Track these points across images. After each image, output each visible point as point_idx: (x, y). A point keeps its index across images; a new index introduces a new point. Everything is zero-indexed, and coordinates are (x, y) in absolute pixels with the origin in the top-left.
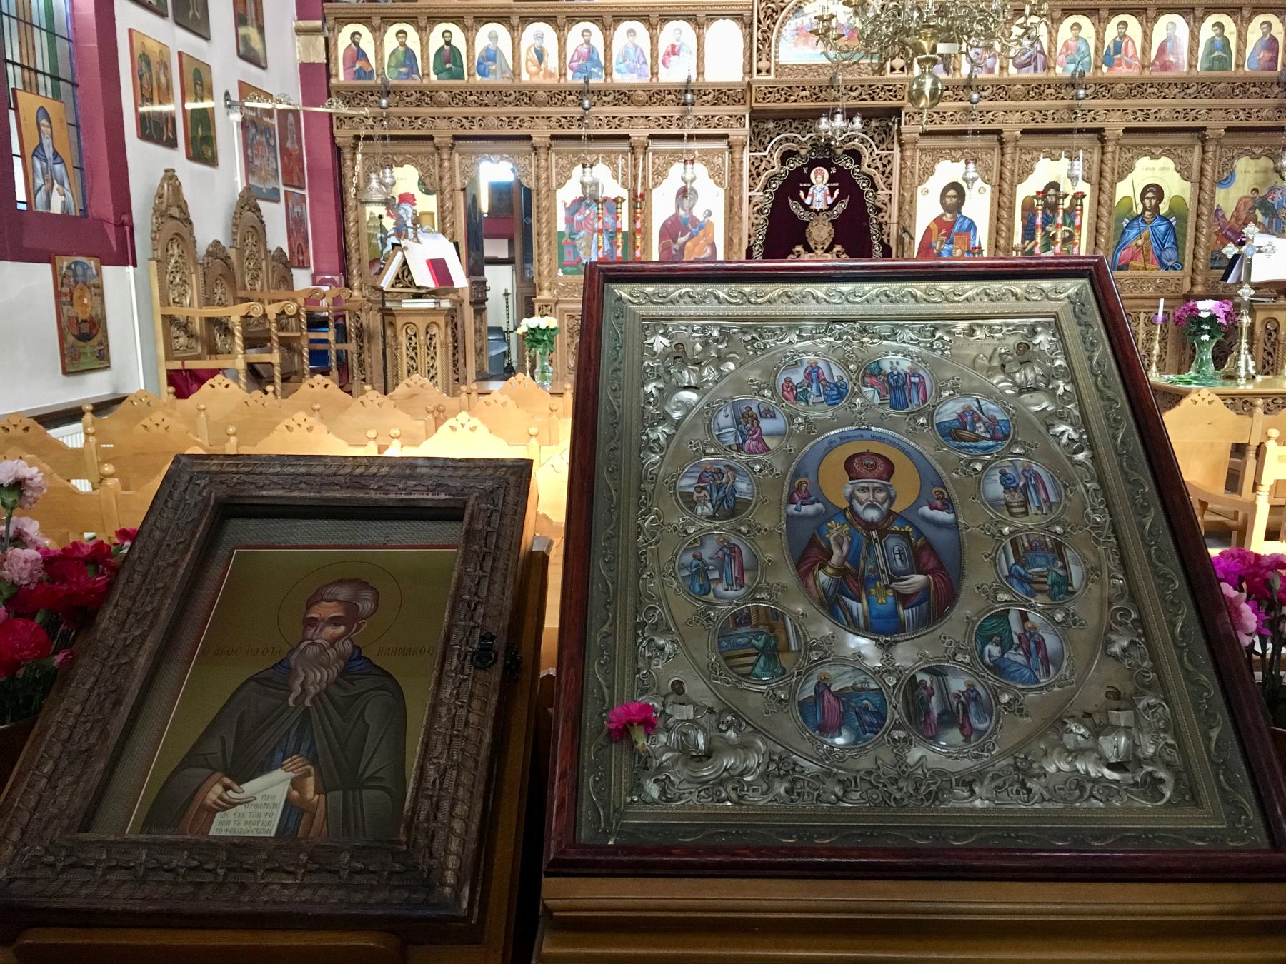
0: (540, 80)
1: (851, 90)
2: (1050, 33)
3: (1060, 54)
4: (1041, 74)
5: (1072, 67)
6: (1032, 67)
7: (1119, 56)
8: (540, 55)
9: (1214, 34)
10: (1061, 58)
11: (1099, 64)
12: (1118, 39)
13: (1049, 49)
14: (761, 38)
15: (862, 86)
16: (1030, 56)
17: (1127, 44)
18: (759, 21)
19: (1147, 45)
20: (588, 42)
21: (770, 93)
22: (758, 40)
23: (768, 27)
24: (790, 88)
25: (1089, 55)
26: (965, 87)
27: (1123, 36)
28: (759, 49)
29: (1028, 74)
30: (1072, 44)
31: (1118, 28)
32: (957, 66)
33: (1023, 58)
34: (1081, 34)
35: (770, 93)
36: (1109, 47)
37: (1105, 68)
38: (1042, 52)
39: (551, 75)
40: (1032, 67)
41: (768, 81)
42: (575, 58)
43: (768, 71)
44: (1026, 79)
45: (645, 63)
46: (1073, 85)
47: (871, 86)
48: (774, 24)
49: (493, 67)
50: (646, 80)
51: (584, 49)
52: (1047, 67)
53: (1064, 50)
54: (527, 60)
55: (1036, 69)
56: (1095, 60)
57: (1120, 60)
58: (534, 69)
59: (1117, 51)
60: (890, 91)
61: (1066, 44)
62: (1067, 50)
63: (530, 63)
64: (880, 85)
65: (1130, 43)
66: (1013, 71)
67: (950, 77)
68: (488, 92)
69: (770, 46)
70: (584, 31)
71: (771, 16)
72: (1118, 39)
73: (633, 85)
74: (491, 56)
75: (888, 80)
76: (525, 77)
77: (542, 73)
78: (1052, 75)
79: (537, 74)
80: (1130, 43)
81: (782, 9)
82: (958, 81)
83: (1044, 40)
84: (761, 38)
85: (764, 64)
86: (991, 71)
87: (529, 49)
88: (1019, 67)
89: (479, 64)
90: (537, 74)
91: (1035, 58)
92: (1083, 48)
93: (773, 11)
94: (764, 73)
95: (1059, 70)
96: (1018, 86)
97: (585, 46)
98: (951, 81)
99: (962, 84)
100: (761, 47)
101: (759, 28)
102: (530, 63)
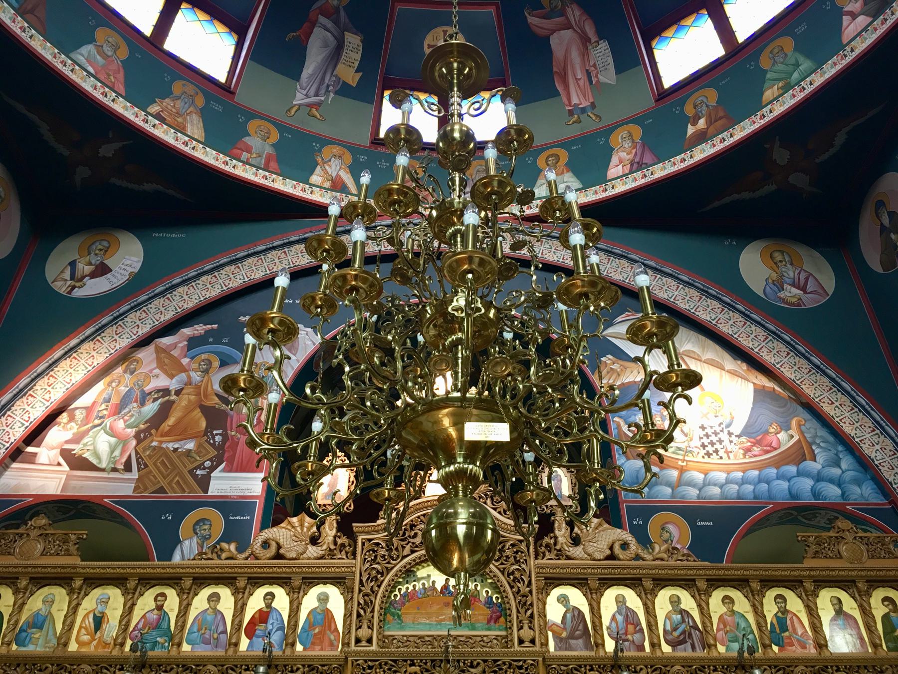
0: (91, 650)
1: (472, 666)
2: (699, 606)
3: (718, 630)
4: (700, 653)
5: (736, 646)
6: (688, 645)
7: (787, 634)
8: (99, 622)
9: (887, 610)
10: (720, 635)
11: (767, 642)
12: (780, 614)
13: (703, 623)
14: (362, 602)
15: (485, 661)
16: (684, 632)
17: (792, 619)
18: (361, 581)
19: (816, 621)
20: (160, 608)
21: (370, 668)
22: (359, 604)
23: (372, 589)
24: (395, 661)
25: (752, 632)
26: (613, 667)
27: (785, 611)
28: (359, 615)
29: (685, 652)
30: (729, 618)
31: (776, 603)
32: (600, 642)
33: (676, 634)
34: (735, 608)
35: (370, 668)
36: (772, 622)
37: (775, 648)
38: (696, 627)
39: (107, 644)
40: (688, 645)
41: (367, 653)
42: (140, 626)
43: (370, 641)
44: (685, 659)
45: (225, 632)
46: (743, 667)
47: (495, 661)
48: (379, 586)
49: (37, 636)
50: (220, 652)
51: (153, 616)
52: (706, 645)
53: (722, 626)
54: (81, 627)
55: (693, 648)
56: (761, 638)
57: (789, 637)
58: (86, 638)
59: (784, 627)
60: (520, 668)
61: (721, 618)
62: (725, 626)
63: (83, 631)
64: (507, 659)
65: (794, 618)
66: (666, 649)
67: (592, 654)
68: (18, 665)
69: (373, 611)
70: (158, 596)
71: (376, 577)
72: (780, 614)
73: (202, 658)
74: (39, 622)
75: (516, 653)
76: (73, 647)
77: (95, 643)
78: (714, 654)
79: (88, 644)
80: (794, 618)
81: (389, 570)
82: (603, 659)
83: (696, 614)
84: (362, 602)
85: (364, 632)
86: (641, 648)
87: (87, 615)
88: (674, 644)
89: (21, 630)
90: (88, 644)
91: (690, 635)
92: (743, 625)
93: (378, 572)
94: (364, 643)
95: (722, 649)
96: (677, 667)
97: (156, 612)
98: (593, 659)
99: (609, 663)
100: (362, 612)
101: (360, 591)
102: (83, 631)
